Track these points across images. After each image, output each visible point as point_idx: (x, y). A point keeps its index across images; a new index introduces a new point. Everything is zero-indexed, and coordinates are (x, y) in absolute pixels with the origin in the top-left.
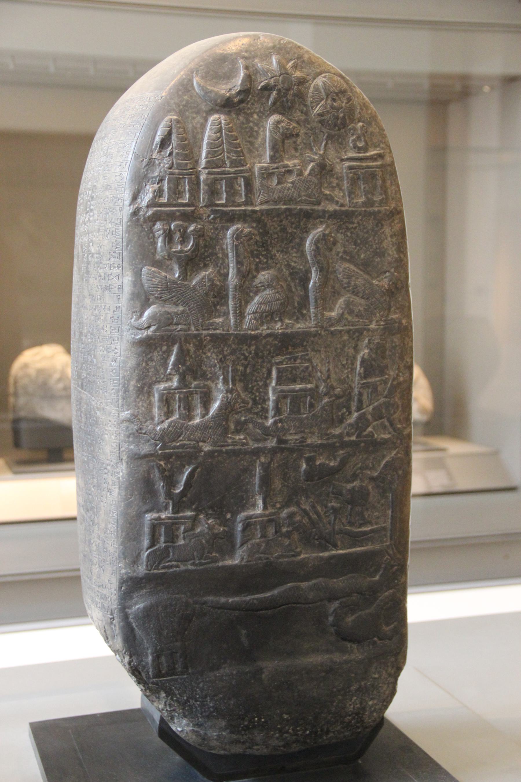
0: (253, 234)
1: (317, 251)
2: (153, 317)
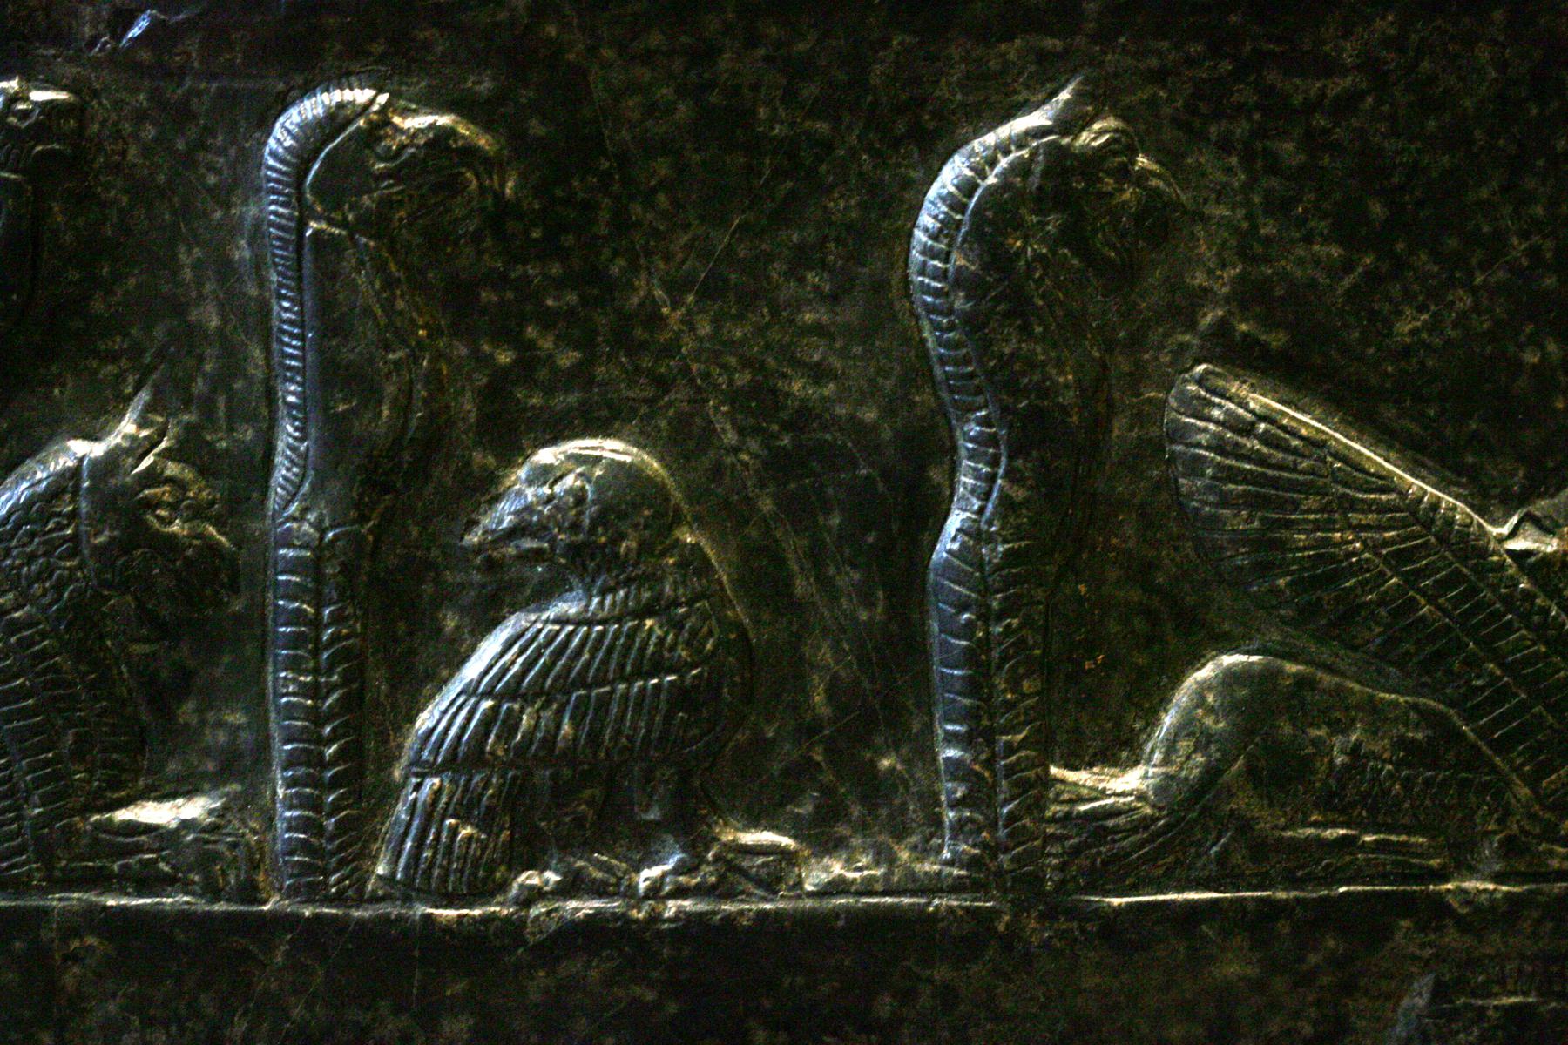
0: (469, 153)
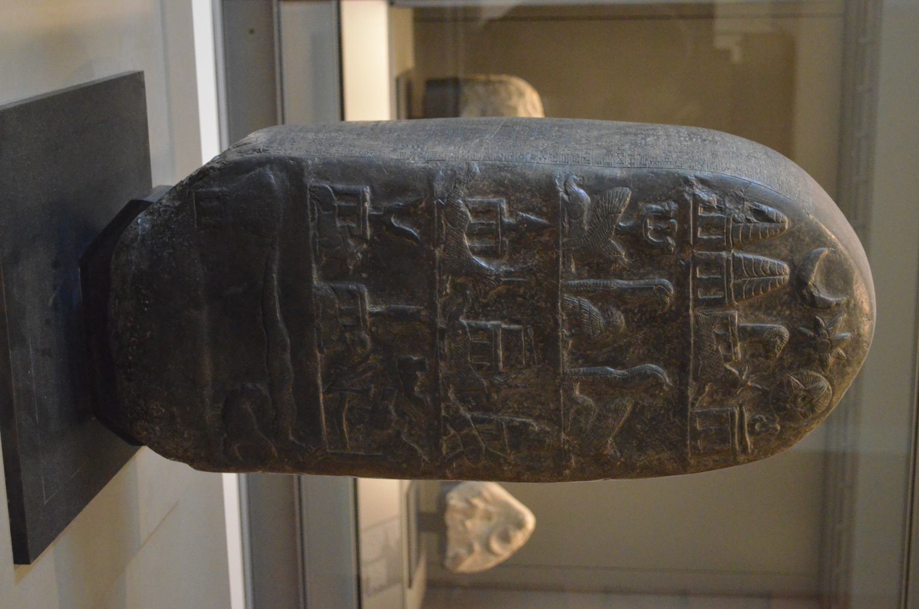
0: (663, 307)
1: (644, 376)
2: (578, 197)
